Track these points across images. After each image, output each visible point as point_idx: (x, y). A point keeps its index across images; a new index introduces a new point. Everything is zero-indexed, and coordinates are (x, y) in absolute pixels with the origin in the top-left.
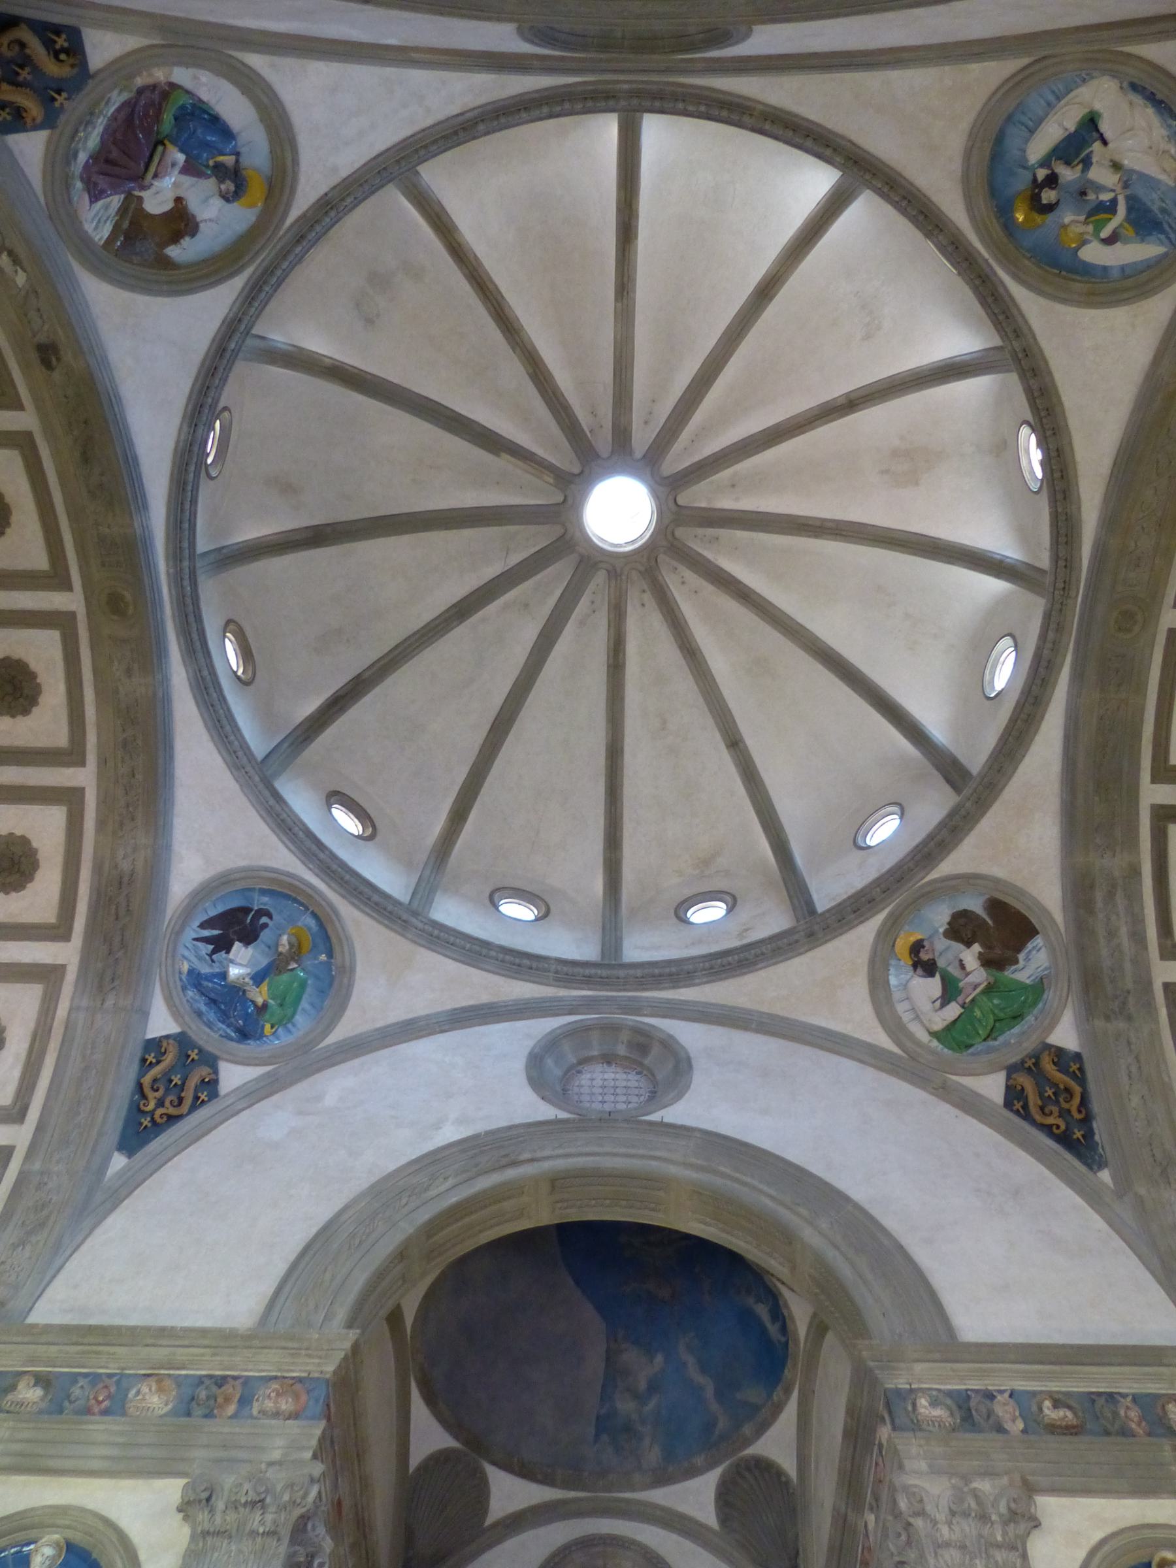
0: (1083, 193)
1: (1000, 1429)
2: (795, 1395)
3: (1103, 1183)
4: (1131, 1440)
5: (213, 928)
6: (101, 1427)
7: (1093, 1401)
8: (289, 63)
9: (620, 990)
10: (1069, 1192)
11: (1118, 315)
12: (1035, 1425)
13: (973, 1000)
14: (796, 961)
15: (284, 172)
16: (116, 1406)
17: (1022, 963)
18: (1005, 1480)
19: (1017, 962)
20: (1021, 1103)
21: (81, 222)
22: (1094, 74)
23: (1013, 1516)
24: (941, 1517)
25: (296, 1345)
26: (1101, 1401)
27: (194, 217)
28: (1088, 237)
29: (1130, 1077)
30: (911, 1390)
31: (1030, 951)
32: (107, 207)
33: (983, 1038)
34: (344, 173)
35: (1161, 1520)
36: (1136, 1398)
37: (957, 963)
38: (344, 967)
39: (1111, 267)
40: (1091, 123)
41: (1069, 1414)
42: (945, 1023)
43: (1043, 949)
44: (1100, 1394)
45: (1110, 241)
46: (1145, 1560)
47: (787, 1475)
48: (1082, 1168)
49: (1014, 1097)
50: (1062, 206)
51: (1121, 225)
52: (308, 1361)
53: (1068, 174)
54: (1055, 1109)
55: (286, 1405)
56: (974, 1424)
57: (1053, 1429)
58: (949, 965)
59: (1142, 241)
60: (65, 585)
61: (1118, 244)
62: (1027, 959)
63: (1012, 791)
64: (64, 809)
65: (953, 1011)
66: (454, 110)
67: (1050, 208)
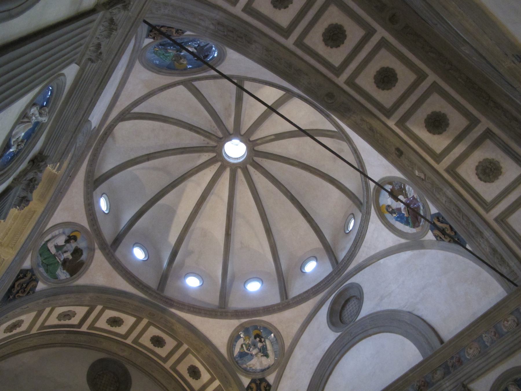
0: (254, 345)
5: (207, 48)
8: (397, 243)
9: (96, 143)
11: (226, 340)
13: (56, 258)
14: (83, 200)
15: (383, 219)
17: (63, 271)
19: (64, 270)
20: (22, 276)
21: (413, 189)
22: (275, 361)
27: (392, 198)
28: (245, 341)
29: (25, 308)
31: (66, 274)
32: (410, 194)
33: (43, 261)
34: (370, 223)
37: (67, 250)
38: (161, 72)
39: (236, 343)
40: (266, 355)
42: (50, 248)
43: (66, 278)
45: (242, 346)
49: (24, 273)
50: (254, 339)
51: (244, 350)
53: (260, 345)
54: (19, 288)
58: (67, 247)
59: (239, 352)
60: (347, 82)
61: (240, 347)
62: (64, 272)
63: (115, 274)
64: (285, 27)
65: (53, 251)
66: (361, 250)
67: (255, 338)
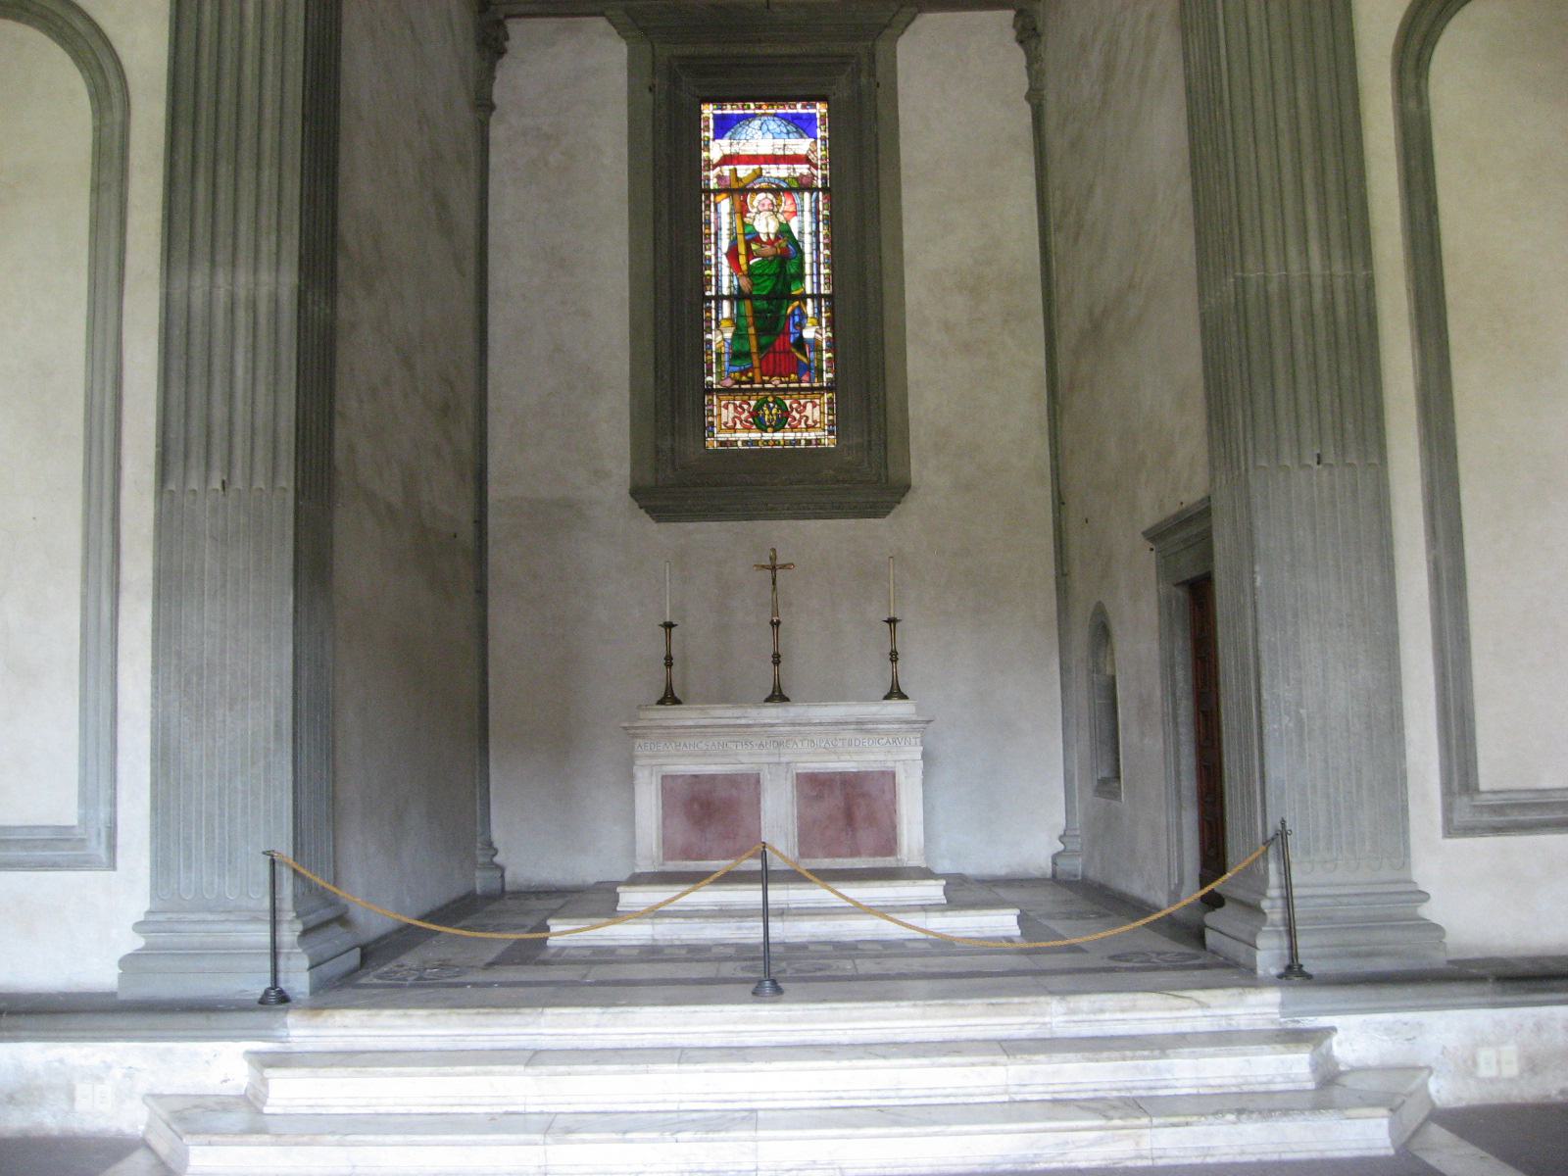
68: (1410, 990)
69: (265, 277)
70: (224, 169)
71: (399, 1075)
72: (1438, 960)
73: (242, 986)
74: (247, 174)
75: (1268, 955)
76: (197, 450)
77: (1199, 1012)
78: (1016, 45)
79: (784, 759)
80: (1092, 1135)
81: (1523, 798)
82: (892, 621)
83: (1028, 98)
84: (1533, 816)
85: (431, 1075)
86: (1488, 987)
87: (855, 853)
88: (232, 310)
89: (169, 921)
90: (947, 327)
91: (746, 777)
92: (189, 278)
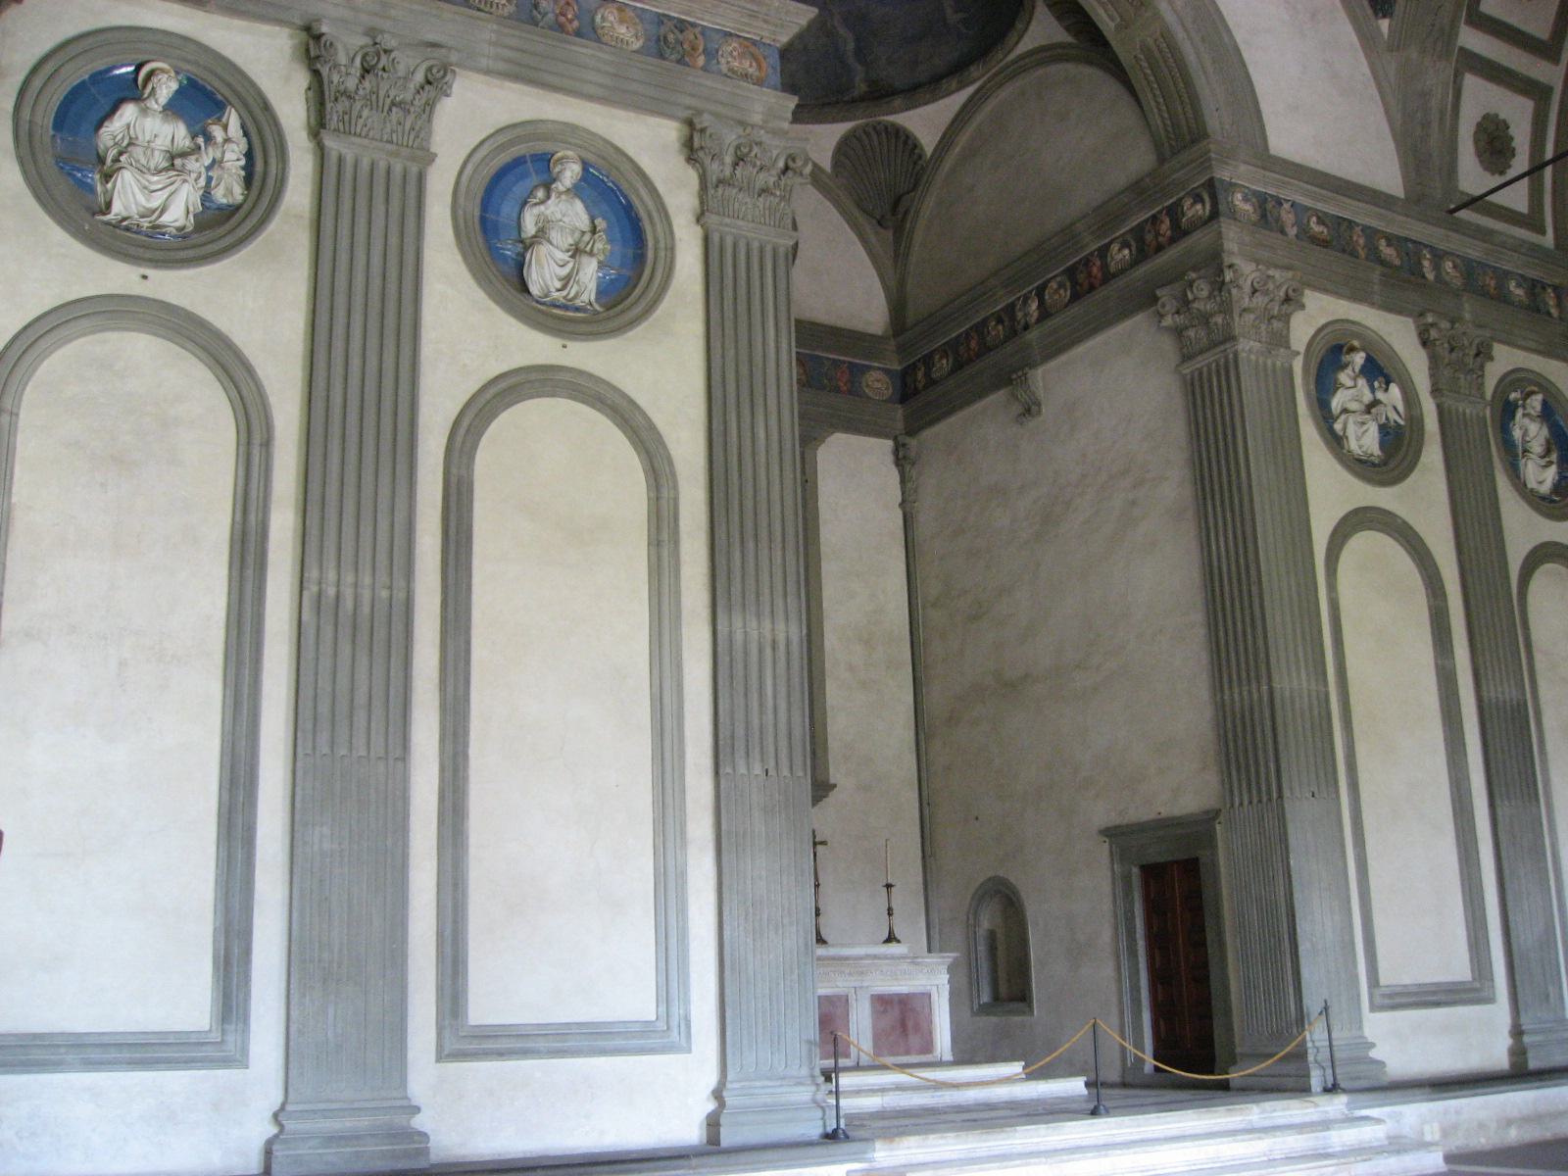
1: (1283, 232)
2: (971, 90)
3: (1378, 28)
4: (1353, 259)
6: (590, 51)
7: (1339, 224)
10: (1349, 28)
12: (1305, 234)
16: (589, 32)
18: (1290, 274)
23: (1287, 299)
24: (1247, 289)
25: (755, 8)
26: (1345, 224)
30: (1235, 184)
35: (1357, 319)
36: (1365, 229)
41: (1325, 231)
44: (1345, 219)
46: (1342, 342)
47: (922, 149)
48: (1370, 11)
52: (765, 26)
55: (747, 66)
56: (1267, 222)
57: (1315, 240)
68: (1398, 1093)
69: (781, 626)
70: (751, 545)
71: (981, 1170)
72: (1385, 1080)
73: (802, 1131)
74: (764, 553)
75: (1316, 1081)
76: (740, 745)
77: (1313, 1110)
78: (893, 466)
79: (865, 984)
80: (1331, 1169)
81: (1399, 990)
82: (889, 886)
83: (902, 504)
84: (1404, 1000)
85: (999, 1168)
86: (1427, 1090)
87: (907, 1053)
88: (761, 651)
89: (742, 1088)
90: (851, 668)
91: (839, 997)
92: (773, 623)
